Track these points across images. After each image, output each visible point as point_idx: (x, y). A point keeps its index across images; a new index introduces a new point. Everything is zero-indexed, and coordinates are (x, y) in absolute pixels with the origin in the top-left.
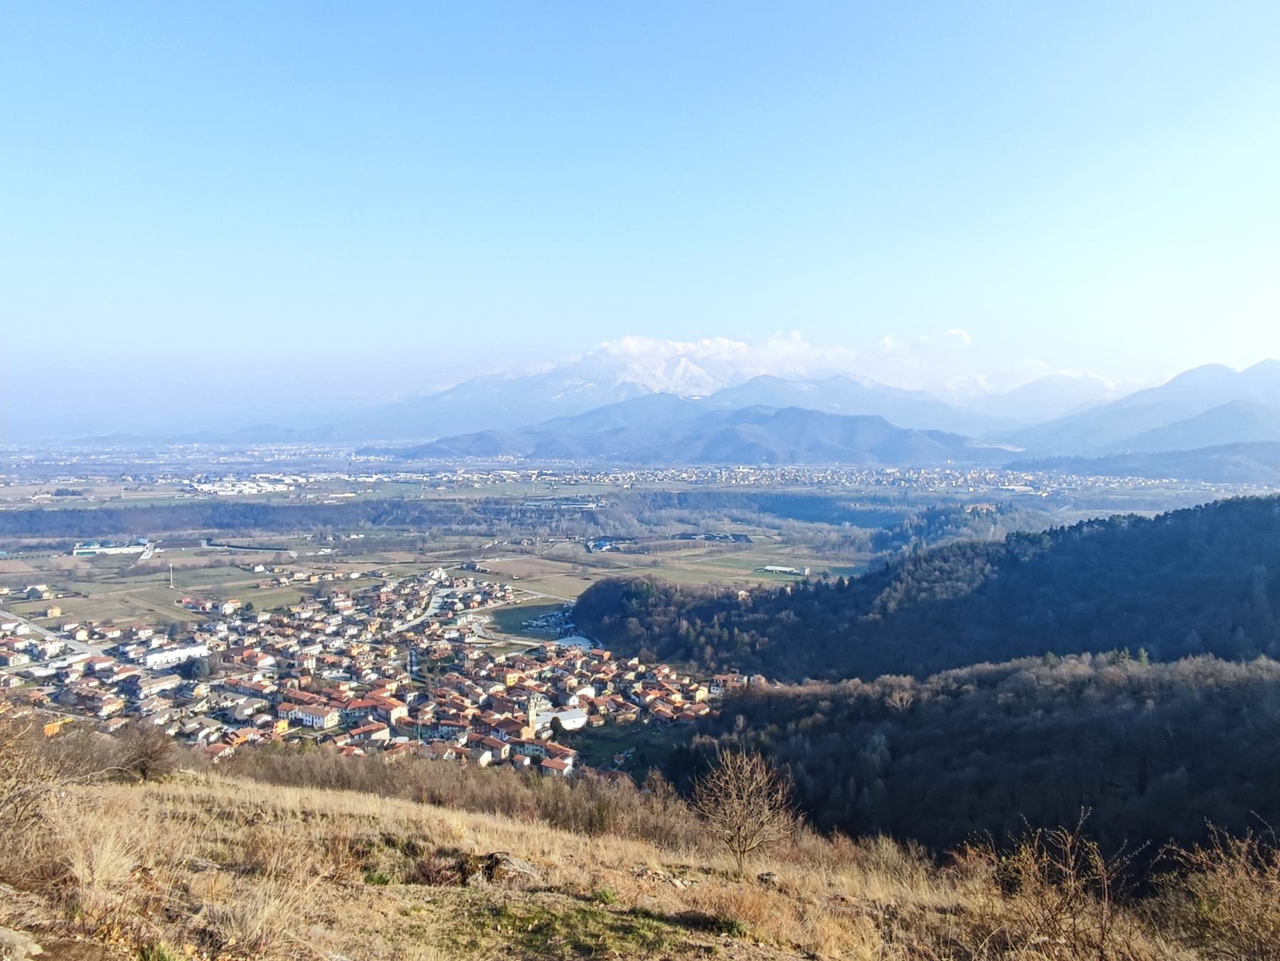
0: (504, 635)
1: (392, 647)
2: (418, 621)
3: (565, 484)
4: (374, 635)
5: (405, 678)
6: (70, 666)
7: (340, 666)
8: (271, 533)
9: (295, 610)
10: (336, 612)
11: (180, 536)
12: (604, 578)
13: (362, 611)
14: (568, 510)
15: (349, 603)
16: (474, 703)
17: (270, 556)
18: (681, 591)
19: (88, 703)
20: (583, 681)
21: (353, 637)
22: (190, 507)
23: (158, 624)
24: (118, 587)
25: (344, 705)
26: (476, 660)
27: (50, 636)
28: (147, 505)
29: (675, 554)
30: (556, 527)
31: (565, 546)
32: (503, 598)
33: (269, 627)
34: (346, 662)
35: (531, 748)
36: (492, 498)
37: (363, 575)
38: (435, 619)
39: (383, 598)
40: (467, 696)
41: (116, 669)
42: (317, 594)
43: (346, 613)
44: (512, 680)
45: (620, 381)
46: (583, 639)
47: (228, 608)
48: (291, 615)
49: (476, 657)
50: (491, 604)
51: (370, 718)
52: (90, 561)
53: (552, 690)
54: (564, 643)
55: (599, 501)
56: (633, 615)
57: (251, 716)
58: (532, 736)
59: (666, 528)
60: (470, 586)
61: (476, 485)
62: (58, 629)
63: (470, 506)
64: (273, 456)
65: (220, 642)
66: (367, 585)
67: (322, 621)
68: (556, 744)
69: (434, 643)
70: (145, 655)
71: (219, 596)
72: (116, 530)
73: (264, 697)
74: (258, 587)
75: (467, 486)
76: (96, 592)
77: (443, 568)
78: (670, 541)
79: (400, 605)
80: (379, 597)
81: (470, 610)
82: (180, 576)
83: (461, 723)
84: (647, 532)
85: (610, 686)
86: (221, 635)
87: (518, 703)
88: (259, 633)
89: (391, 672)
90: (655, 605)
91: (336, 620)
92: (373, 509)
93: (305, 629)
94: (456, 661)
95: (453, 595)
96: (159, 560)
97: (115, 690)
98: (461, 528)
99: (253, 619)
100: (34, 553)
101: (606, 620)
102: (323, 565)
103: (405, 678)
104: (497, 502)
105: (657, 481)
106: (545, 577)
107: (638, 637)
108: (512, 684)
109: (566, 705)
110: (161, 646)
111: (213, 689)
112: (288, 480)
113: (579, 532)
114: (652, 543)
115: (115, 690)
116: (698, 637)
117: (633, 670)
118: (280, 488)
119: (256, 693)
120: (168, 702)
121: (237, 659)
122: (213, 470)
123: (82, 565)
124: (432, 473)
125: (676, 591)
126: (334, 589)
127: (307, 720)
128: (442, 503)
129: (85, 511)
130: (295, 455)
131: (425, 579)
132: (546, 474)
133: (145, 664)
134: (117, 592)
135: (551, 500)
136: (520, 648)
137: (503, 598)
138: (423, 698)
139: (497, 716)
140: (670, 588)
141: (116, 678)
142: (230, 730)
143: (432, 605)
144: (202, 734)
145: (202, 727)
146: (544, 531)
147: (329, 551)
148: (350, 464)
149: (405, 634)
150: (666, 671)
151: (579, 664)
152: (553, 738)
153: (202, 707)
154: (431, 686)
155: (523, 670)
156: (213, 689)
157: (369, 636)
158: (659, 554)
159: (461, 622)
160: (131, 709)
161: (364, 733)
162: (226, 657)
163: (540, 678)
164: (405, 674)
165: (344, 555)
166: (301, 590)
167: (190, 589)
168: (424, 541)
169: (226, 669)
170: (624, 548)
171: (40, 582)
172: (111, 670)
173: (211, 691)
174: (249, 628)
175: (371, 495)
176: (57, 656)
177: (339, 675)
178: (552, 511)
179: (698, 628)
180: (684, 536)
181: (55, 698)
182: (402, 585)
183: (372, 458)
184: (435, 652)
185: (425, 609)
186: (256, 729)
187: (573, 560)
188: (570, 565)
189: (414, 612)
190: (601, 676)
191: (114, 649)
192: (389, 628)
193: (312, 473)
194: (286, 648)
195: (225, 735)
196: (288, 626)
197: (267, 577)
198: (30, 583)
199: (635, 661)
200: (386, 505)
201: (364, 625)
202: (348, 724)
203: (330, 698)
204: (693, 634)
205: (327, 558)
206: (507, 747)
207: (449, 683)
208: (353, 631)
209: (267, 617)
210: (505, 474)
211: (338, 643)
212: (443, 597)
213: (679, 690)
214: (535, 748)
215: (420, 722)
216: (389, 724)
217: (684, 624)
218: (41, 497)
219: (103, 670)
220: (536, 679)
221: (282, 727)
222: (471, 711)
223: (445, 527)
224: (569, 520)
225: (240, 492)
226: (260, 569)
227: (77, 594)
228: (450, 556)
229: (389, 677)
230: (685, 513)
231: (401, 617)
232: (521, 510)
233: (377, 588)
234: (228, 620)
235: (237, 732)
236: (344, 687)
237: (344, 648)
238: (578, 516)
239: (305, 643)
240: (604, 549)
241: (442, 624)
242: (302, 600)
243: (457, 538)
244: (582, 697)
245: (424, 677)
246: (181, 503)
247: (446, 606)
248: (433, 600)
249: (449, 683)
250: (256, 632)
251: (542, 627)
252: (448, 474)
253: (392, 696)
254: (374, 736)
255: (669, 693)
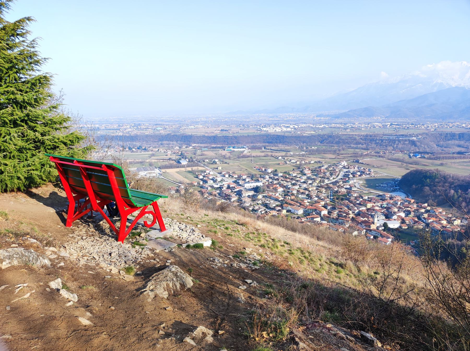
0: (368, 189)
1: (324, 189)
2: (334, 180)
3: (403, 129)
4: (318, 184)
5: (328, 200)
6: (223, 185)
7: (305, 194)
8: (285, 146)
9: (291, 173)
10: (305, 175)
11: (256, 146)
12: (415, 169)
13: (314, 175)
14: (403, 140)
15: (310, 172)
16: (353, 213)
17: (283, 154)
18: (453, 177)
19: (227, 197)
20: (400, 210)
21: (310, 184)
22: (260, 136)
23: (248, 174)
24: (237, 161)
25: (305, 207)
26: (355, 197)
27: (218, 175)
28: (246, 135)
29: (453, 161)
30: (396, 147)
31: (400, 155)
32: (369, 174)
33: (282, 178)
34: (307, 192)
35: (374, 232)
36: (369, 134)
37: (315, 162)
38: (341, 180)
39: (322, 171)
40: (351, 210)
41: (236, 187)
42: (299, 168)
43: (308, 175)
44: (369, 206)
45: (435, 82)
46: (403, 193)
47: (269, 171)
48: (289, 175)
49: (356, 196)
50: (364, 176)
51: (314, 213)
52: (230, 153)
53: (386, 212)
54: (393, 194)
55: (418, 136)
56: (427, 186)
57: (275, 207)
58: (375, 228)
59: (450, 149)
60: (356, 169)
61: (363, 129)
62: (220, 173)
63: (359, 137)
64: (287, 118)
65: (266, 182)
66: (316, 166)
67: (300, 177)
68: (385, 233)
69: (340, 189)
70: (244, 184)
71: (266, 166)
72: (238, 143)
73: (279, 201)
74: (279, 164)
75: (359, 129)
76: (231, 162)
77: (346, 161)
78: (451, 155)
79: (328, 174)
80: (320, 170)
81: (355, 178)
82: (255, 159)
83: (347, 219)
84: (440, 150)
85: (412, 214)
86: (267, 179)
87: (371, 215)
88: (279, 180)
89: (323, 198)
90: (439, 183)
91: (305, 177)
92: (321, 138)
93: (294, 180)
94: (348, 197)
95: (349, 172)
96: (249, 153)
97: (235, 194)
98: (355, 146)
99: (277, 175)
100: (215, 149)
101: (414, 186)
102: (301, 158)
103: (328, 200)
104: (371, 136)
105: (448, 128)
106: (388, 167)
107: (428, 195)
108: (369, 208)
109: (391, 218)
110: (249, 181)
111: (264, 197)
112: (291, 127)
113: (407, 149)
114: (442, 156)
115: (235, 194)
116: (459, 198)
117: (424, 208)
118: (289, 129)
119: (276, 200)
120: (250, 199)
121: (271, 188)
122: (267, 123)
123: (227, 154)
124: (345, 124)
125: (450, 177)
126: (305, 166)
127: (292, 211)
128: (348, 136)
129: (229, 136)
130: (294, 117)
131: (338, 165)
132: (394, 125)
133: (244, 186)
134: (237, 163)
135: (395, 135)
136: (374, 194)
137: (369, 174)
138: (334, 208)
139: (362, 219)
140: (447, 175)
141: (236, 190)
142: (268, 211)
143: (340, 175)
144: (259, 211)
145: (260, 209)
146: (390, 148)
147: (304, 153)
148: (314, 121)
149: (329, 185)
150: (441, 210)
151: (399, 203)
152: (384, 230)
153: (260, 202)
154: (337, 205)
155: (375, 203)
156: (264, 197)
157: (316, 184)
158: (445, 160)
159: (351, 182)
160: (240, 200)
161: (311, 218)
162: (268, 187)
163: (381, 207)
164: (328, 199)
165: (309, 154)
166: (294, 166)
167: (258, 163)
168: (339, 150)
169: (268, 191)
170: (428, 157)
171: (216, 158)
172: (234, 187)
173: (263, 197)
174: (276, 178)
175: (321, 132)
176: (220, 182)
177: (304, 197)
178: (395, 140)
179: (459, 194)
180: (459, 153)
181: (219, 194)
182: (329, 167)
183: (322, 118)
184: (340, 192)
185: (338, 176)
186: (276, 211)
187: (402, 161)
188: (400, 163)
189: (333, 177)
190: (409, 209)
191: (235, 181)
192: (323, 182)
193: (300, 124)
194: (287, 186)
195: (266, 212)
196: (288, 178)
197: (282, 161)
198: (214, 159)
199: (426, 205)
200: (326, 136)
201: (314, 180)
202: (306, 214)
203: (301, 205)
204: (456, 196)
205: (303, 155)
206: (365, 231)
207: (344, 204)
208: (310, 182)
209: (281, 174)
210: (376, 125)
211: (305, 186)
212: (345, 172)
213: (446, 219)
214: (376, 233)
215: (332, 217)
216: (321, 216)
217: (452, 191)
218: (216, 131)
219: (232, 187)
220: (379, 207)
221: (284, 212)
222: (351, 215)
223: (348, 145)
224: (402, 144)
225: (275, 131)
226: (280, 158)
227: (226, 163)
228: (349, 157)
229: (322, 199)
230: (462, 143)
231: (328, 178)
232: (381, 139)
233: (320, 167)
234: (269, 175)
235: (270, 212)
236: (306, 201)
237: (307, 187)
238: (407, 142)
239: (294, 184)
240: (418, 157)
241: (343, 182)
242: (294, 170)
243: (353, 150)
244: (399, 216)
245: (335, 201)
246: (256, 134)
247: (346, 176)
248: (341, 173)
249: (344, 204)
250: (278, 179)
251: (385, 187)
252: (351, 124)
253: (322, 206)
254: (315, 219)
255: (440, 220)
